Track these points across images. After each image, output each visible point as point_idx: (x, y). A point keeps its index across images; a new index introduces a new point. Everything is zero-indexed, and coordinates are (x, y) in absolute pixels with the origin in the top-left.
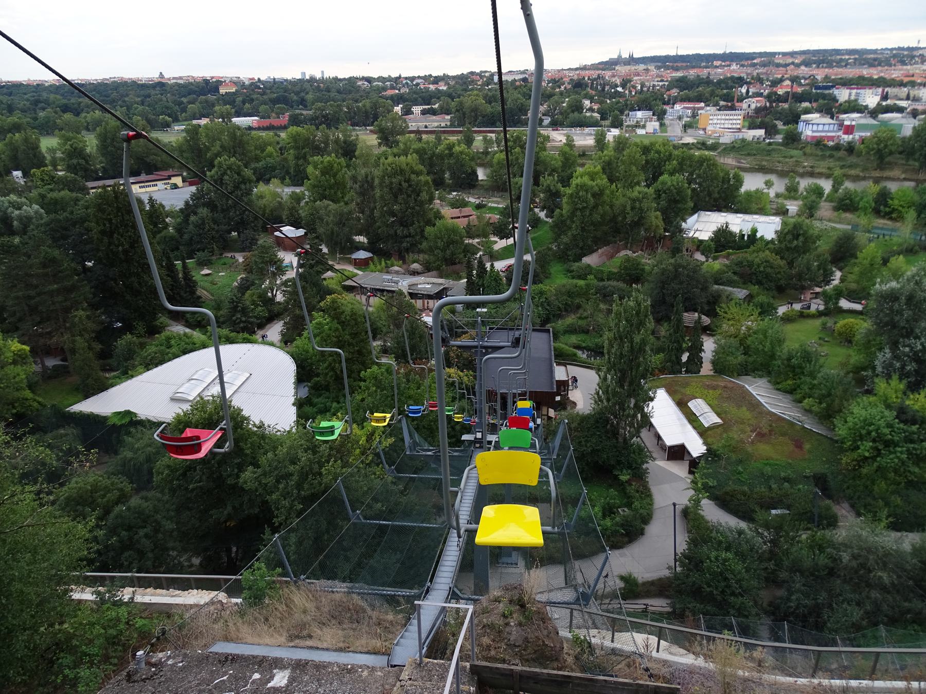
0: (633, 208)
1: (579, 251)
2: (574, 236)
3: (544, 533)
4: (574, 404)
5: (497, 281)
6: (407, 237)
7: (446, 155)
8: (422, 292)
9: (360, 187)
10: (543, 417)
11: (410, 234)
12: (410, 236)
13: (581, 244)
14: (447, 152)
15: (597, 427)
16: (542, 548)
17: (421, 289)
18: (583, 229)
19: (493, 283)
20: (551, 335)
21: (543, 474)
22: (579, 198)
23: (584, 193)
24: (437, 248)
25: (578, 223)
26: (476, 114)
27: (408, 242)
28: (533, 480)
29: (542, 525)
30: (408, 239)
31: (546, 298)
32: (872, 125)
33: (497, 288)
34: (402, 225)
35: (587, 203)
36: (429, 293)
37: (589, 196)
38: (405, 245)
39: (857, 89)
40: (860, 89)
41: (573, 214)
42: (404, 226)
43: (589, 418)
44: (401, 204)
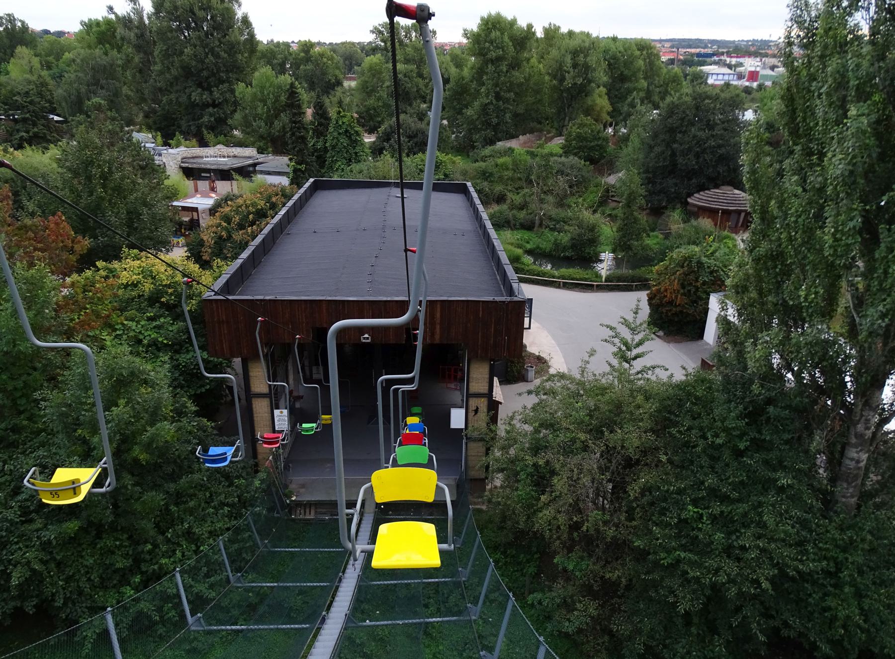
0: (575, 66)
1: (490, 133)
2: (484, 107)
3: (442, 553)
4: (540, 360)
5: (350, 137)
6: (207, 105)
7: (301, 60)
8: (208, 167)
9: (136, 34)
10: (473, 402)
11: (214, 101)
12: (214, 105)
13: (495, 121)
14: (302, 54)
15: (758, 445)
16: (440, 568)
17: (207, 163)
18: (498, 97)
19: (344, 141)
20: (475, 195)
21: (439, 490)
22: (491, 42)
23: (498, 33)
24: (256, 117)
25: (489, 84)
26: (351, 64)
27: (211, 115)
28: (430, 498)
29: (439, 543)
30: (211, 109)
31: (446, 175)
32: (771, 76)
33: (352, 151)
34: (200, 85)
35: (503, 51)
36: (221, 167)
37: (506, 39)
38: (206, 119)
39: (737, 57)
40: (740, 57)
41: (480, 72)
42: (204, 89)
43: (706, 403)
44: (195, 46)
